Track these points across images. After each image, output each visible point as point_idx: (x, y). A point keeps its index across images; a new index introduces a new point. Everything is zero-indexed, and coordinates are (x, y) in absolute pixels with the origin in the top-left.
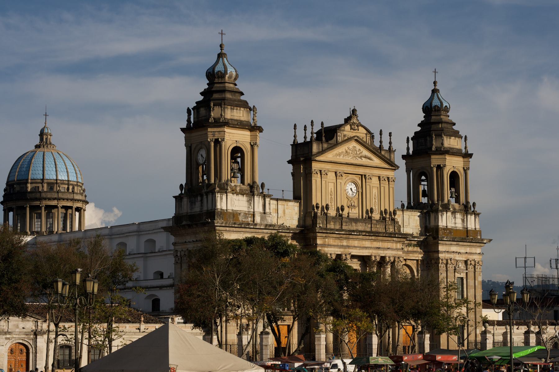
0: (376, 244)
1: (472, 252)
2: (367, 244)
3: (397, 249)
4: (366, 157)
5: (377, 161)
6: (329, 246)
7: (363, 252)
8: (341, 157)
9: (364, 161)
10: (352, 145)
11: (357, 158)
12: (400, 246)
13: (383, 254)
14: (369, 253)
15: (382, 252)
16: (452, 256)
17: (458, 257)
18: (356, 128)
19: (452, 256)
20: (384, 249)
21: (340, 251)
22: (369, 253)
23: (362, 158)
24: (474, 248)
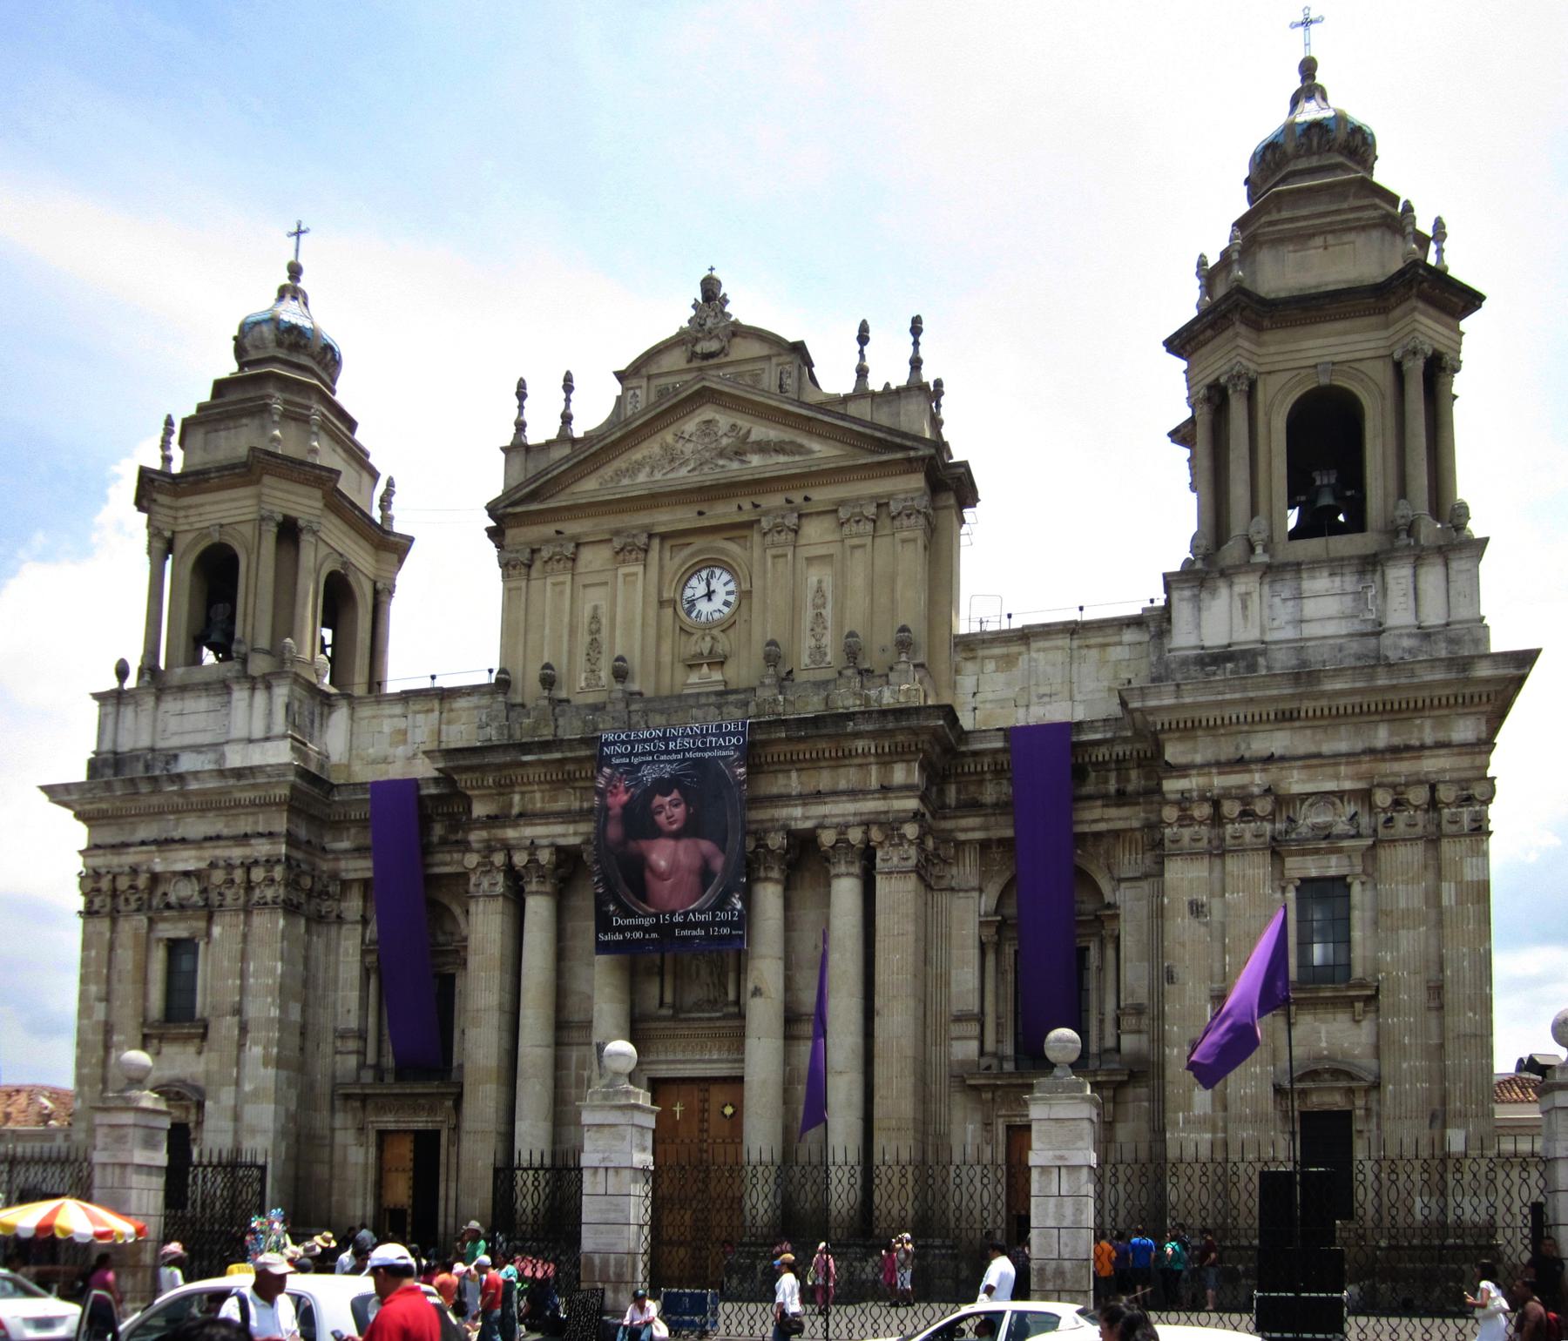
1: (1415, 742)
4: (763, 448)
5: (822, 451)
6: (526, 817)
8: (642, 477)
10: (697, 420)
11: (721, 462)
16: (1257, 779)
17: (1296, 782)
19: (1257, 779)
21: (575, 834)
23: (749, 457)
24: (1428, 724)
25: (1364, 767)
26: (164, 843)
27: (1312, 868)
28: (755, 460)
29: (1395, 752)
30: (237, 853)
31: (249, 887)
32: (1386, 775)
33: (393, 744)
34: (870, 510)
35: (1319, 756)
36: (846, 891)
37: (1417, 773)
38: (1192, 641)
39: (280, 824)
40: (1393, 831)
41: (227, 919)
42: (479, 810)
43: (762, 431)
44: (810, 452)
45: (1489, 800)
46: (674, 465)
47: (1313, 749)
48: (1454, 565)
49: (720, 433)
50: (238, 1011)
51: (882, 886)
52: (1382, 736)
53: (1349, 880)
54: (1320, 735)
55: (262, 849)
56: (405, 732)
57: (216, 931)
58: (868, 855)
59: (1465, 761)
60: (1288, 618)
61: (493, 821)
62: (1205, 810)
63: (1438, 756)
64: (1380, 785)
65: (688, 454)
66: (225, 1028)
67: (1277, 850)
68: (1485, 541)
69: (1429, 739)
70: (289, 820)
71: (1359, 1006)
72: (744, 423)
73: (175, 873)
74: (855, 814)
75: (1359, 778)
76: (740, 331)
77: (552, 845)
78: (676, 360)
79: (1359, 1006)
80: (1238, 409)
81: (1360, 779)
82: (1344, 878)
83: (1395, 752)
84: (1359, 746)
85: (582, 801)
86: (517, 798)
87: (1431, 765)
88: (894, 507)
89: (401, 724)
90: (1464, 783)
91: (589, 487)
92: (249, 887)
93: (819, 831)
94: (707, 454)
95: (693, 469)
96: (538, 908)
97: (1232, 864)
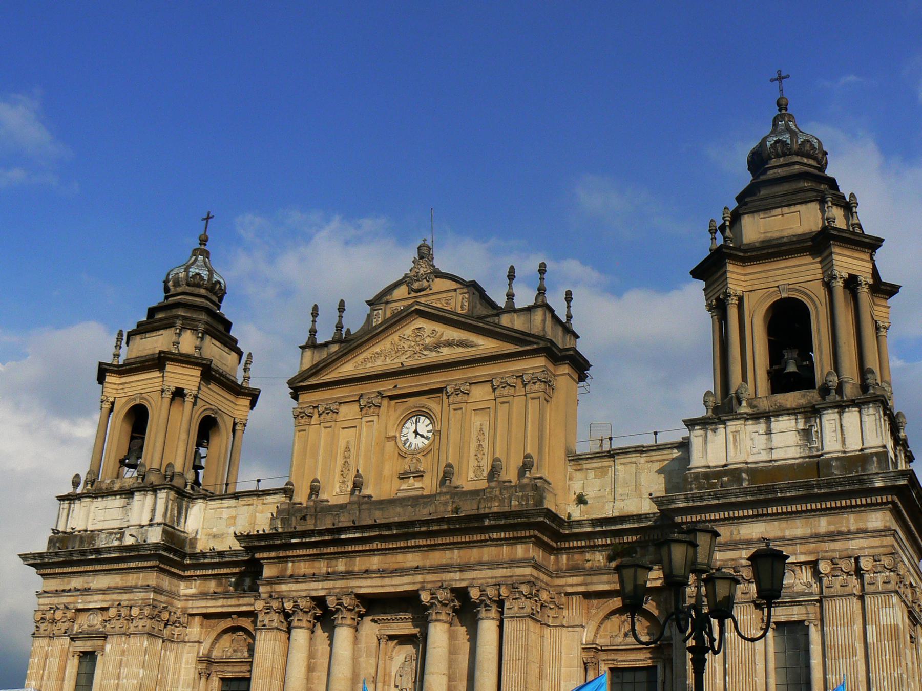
0: (437, 557)
1: (844, 529)
2: (412, 559)
4: (449, 344)
5: (485, 345)
7: (393, 583)
8: (379, 363)
11: (425, 353)
14: (414, 583)
18: (425, 283)
20: (463, 568)
21: (322, 589)
22: (414, 583)
23: (441, 349)
28: (445, 351)
29: (832, 536)
32: (827, 552)
33: (228, 526)
37: (846, 550)
38: (703, 463)
40: (832, 590)
46: (398, 354)
48: (864, 412)
49: (425, 336)
52: (823, 524)
53: (806, 623)
54: (784, 524)
56: (234, 518)
60: (764, 447)
63: (859, 538)
64: (822, 559)
65: (406, 348)
69: (853, 528)
72: (439, 327)
74: (492, 578)
80: (733, 313)
81: (810, 553)
82: (801, 623)
83: (832, 536)
84: (808, 531)
85: (328, 567)
87: (853, 545)
89: (233, 512)
91: (348, 369)
93: (469, 589)
94: (417, 348)
95: (410, 357)
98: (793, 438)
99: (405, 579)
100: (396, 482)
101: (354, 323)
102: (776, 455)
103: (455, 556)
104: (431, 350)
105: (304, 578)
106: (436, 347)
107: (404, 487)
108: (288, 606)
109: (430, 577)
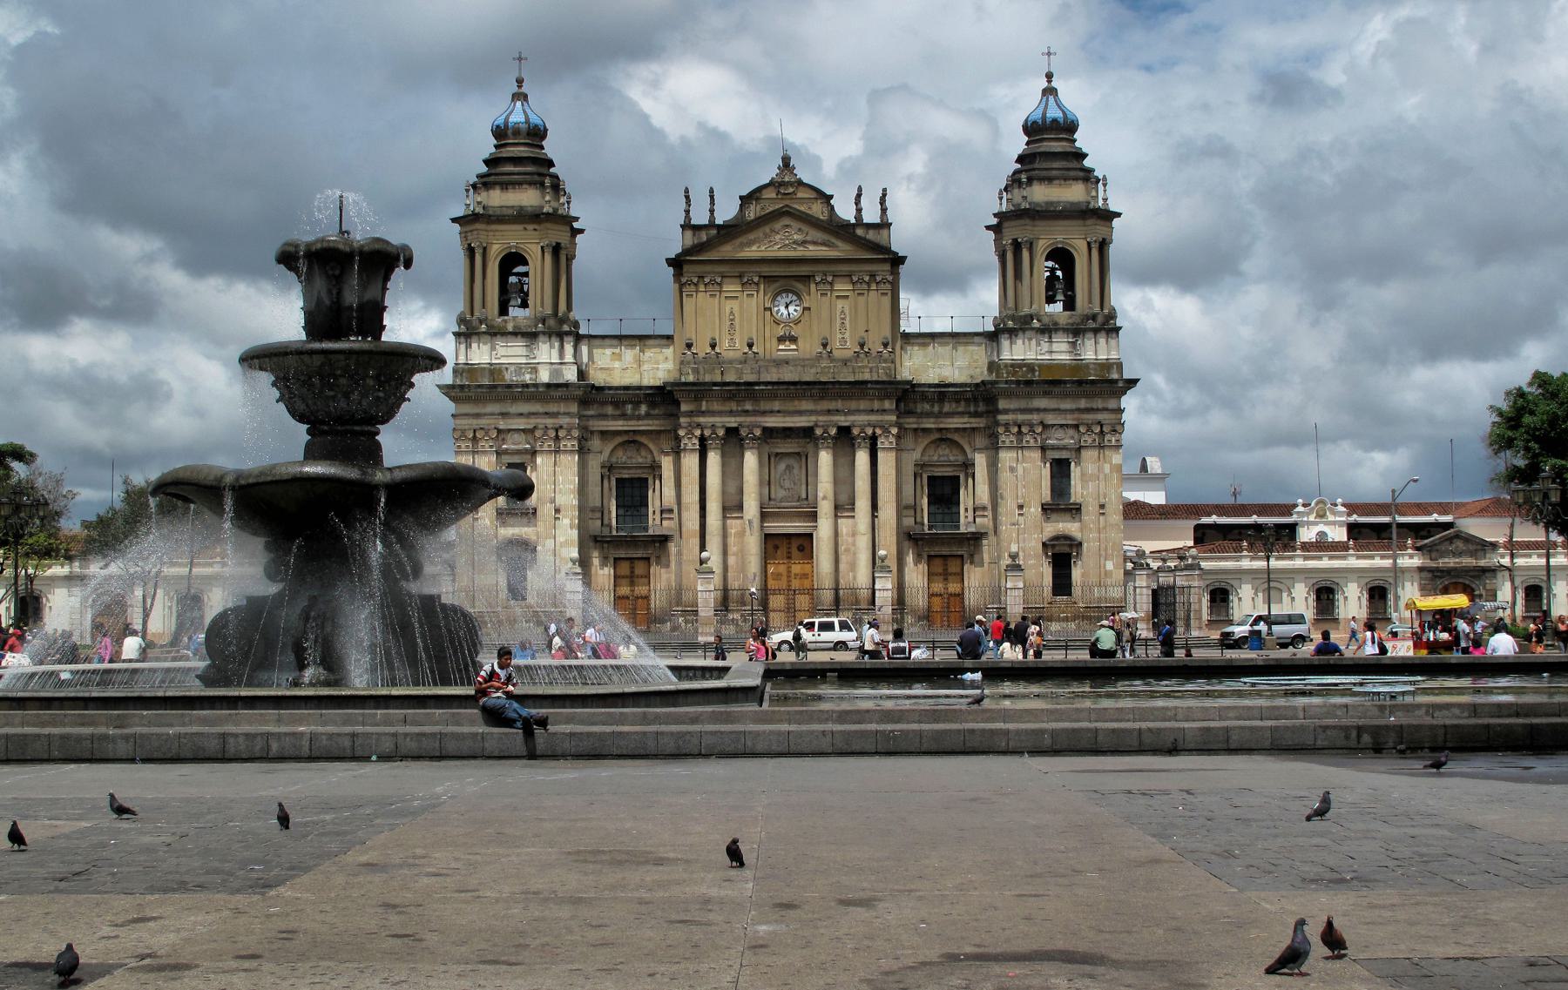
0: (825, 405)
1: (1095, 407)
2: (806, 405)
3: (884, 411)
5: (842, 250)
9: (813, 251)
12: (891, 404)
13: (846, 421)
15: (843, 418)
17: (1050, 419)
19: (1035, 418)
25: (1076, 416)
26: (504, 415)
27: (1057, 455)
28: (811, 248)
30: (549, 422)
31: (557, 438)
34: (867, 279)
35: (1059, 410)
36: (862, 458)
39: (574, 408)
41: (545, 456)
42: (684, 407)
43: (815, 234)
44: (837, 247)
45: (1120, 434)
47: (1056, 406)
50: (553, 501)
51: (880, 455)
52: (1083, 403)
55: (564, 421)
57: (539, 460)
58: (873, 440)
59: (1113, 416)
61: (690, 414)
62: (1015, 430)
64: (1082, 424)
66: (546, 511)
67: (1043, 449)
68: (1120, 328)
69: (1100, 406)
70: (579, 407)
71: (1074, 512)
73: (509, 430)
75: (1074, 420)
76: (800, 183)
77: (723, 426)
78: (770, 194)
79: (1074, 512)
80: (1025, 254)
84: (1074, 406)
86: (704, 403)
88: (878, 279)
90: (1113, 425)
91: (727, 251)
92: (557, 438)
96: (714, 459)
97: (1026, 453)
98: (1064, 347)
99: (804, 418)
100: (775, 341)
101: (726, 212)
102: (1054, 356)
103: (839, 404)
104: (798, 244)
105: (721, 413)
106: (804, 243)
107: (781, 347)
108: (707, 433)
109: (821, 418)
